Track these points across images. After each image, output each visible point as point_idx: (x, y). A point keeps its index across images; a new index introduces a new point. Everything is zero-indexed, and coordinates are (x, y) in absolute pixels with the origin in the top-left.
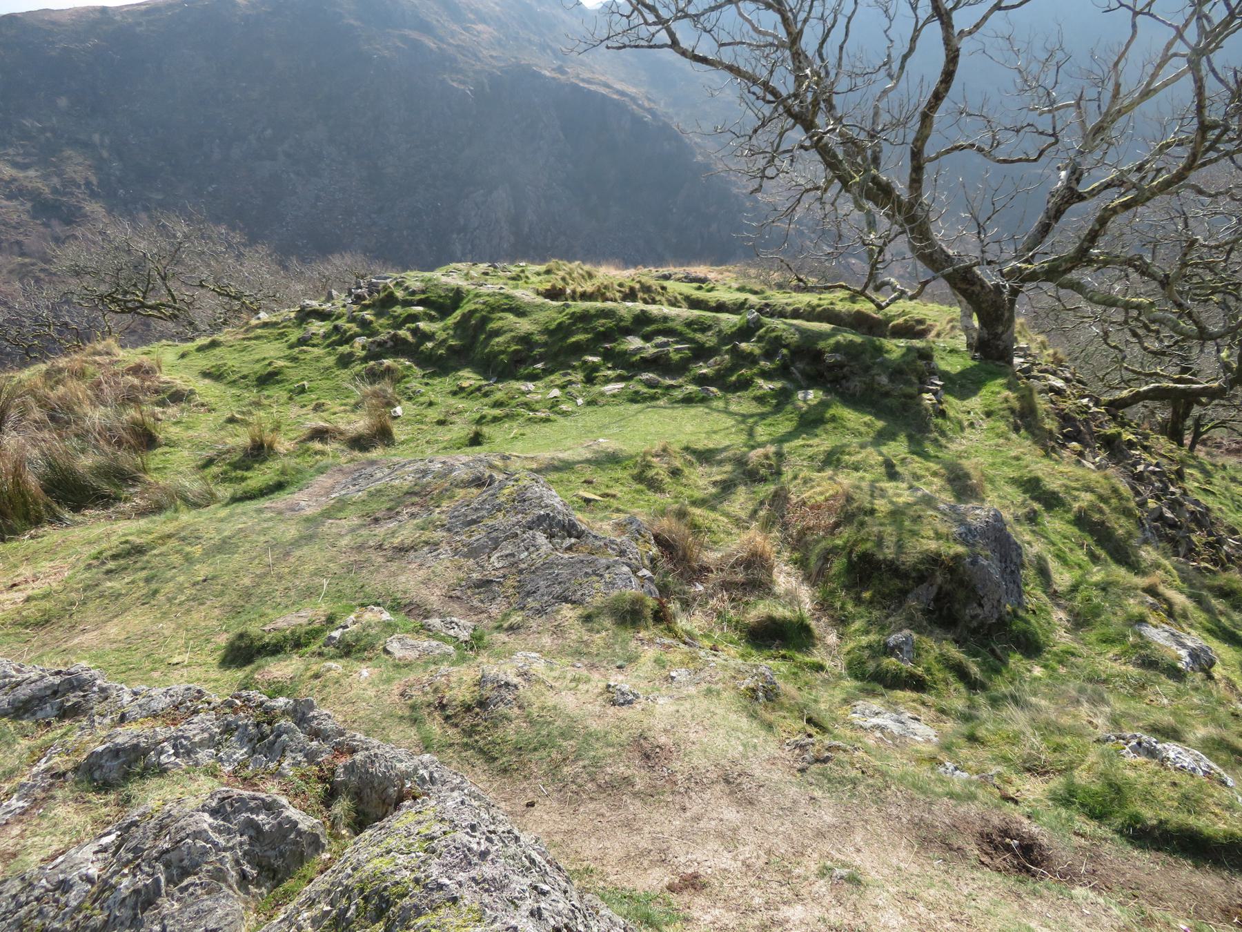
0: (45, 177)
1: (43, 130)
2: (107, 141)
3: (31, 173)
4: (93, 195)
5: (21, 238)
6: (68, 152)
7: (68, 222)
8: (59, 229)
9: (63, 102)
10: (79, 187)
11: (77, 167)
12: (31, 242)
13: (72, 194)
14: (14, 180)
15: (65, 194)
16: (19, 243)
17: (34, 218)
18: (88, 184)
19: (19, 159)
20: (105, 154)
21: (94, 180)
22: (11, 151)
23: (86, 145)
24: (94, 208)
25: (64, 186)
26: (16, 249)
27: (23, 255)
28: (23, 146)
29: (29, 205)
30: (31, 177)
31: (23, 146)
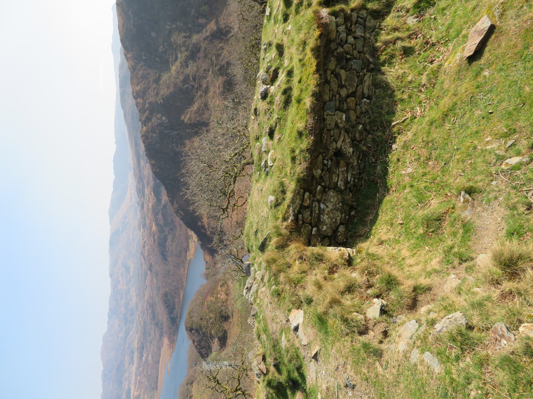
0: (181, 52)
1: (163, 45)
2: (169, 23)
3: (179, 56)
4: (190, 37)
5: (202, 69)
6: (172, 40)
7: (199, 50)
8: (201, 54)
9: (153, 34)
10: (186, 41)
11: (178, 38)
12: (205, 66)
13: (188, 45)
14: (181, 63)
15: (188, 47)
16: (204, 70)
17: (196, 61)
18: (185, 37)
19: (174, 58)
20: (174, 26)
21: (184, 34)
22: (170, 60)
23: (170, 32)
24: (195, 38)
25: (185, 46)
26: (206, 72)
27: (209, 71)
28: (169, 55)
29: (191, 61)
30: (181, 56)
31: (169, 55)
